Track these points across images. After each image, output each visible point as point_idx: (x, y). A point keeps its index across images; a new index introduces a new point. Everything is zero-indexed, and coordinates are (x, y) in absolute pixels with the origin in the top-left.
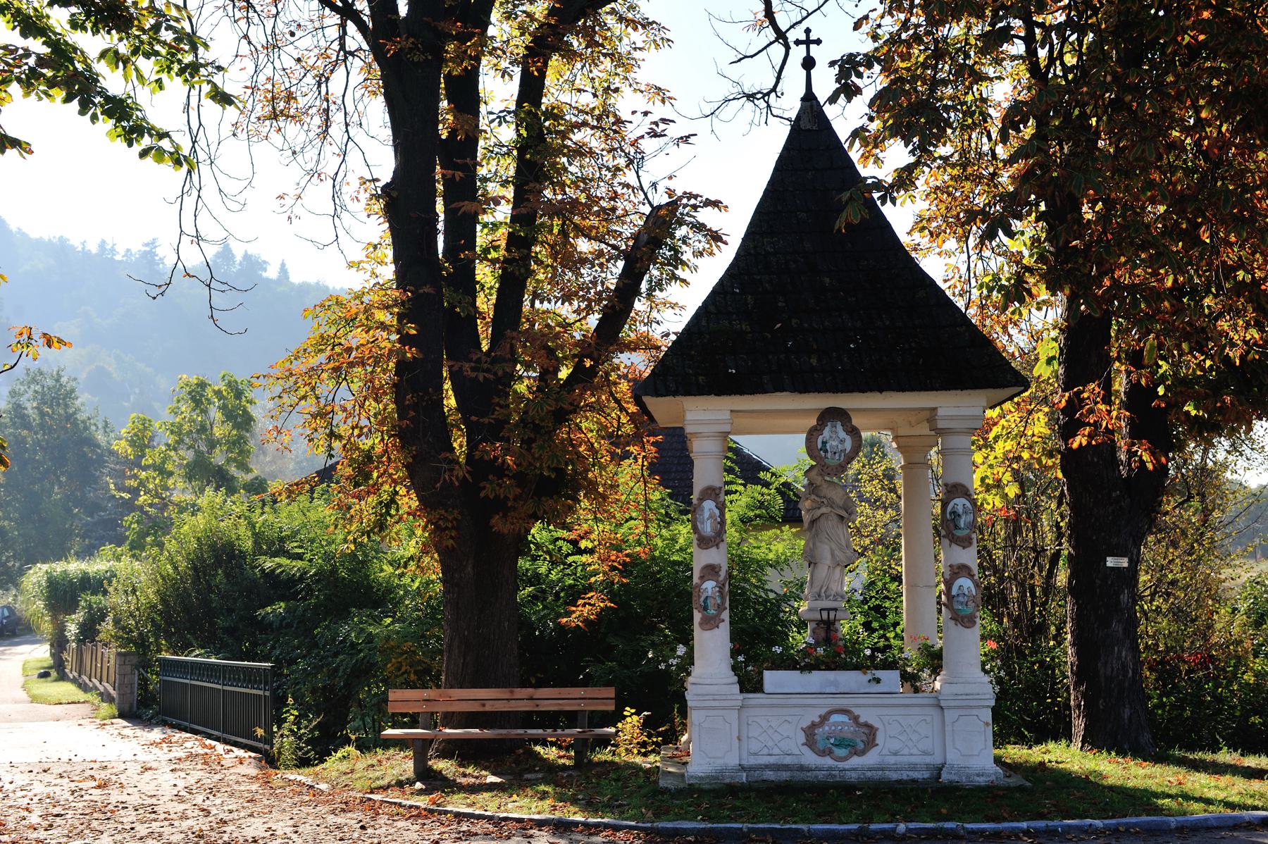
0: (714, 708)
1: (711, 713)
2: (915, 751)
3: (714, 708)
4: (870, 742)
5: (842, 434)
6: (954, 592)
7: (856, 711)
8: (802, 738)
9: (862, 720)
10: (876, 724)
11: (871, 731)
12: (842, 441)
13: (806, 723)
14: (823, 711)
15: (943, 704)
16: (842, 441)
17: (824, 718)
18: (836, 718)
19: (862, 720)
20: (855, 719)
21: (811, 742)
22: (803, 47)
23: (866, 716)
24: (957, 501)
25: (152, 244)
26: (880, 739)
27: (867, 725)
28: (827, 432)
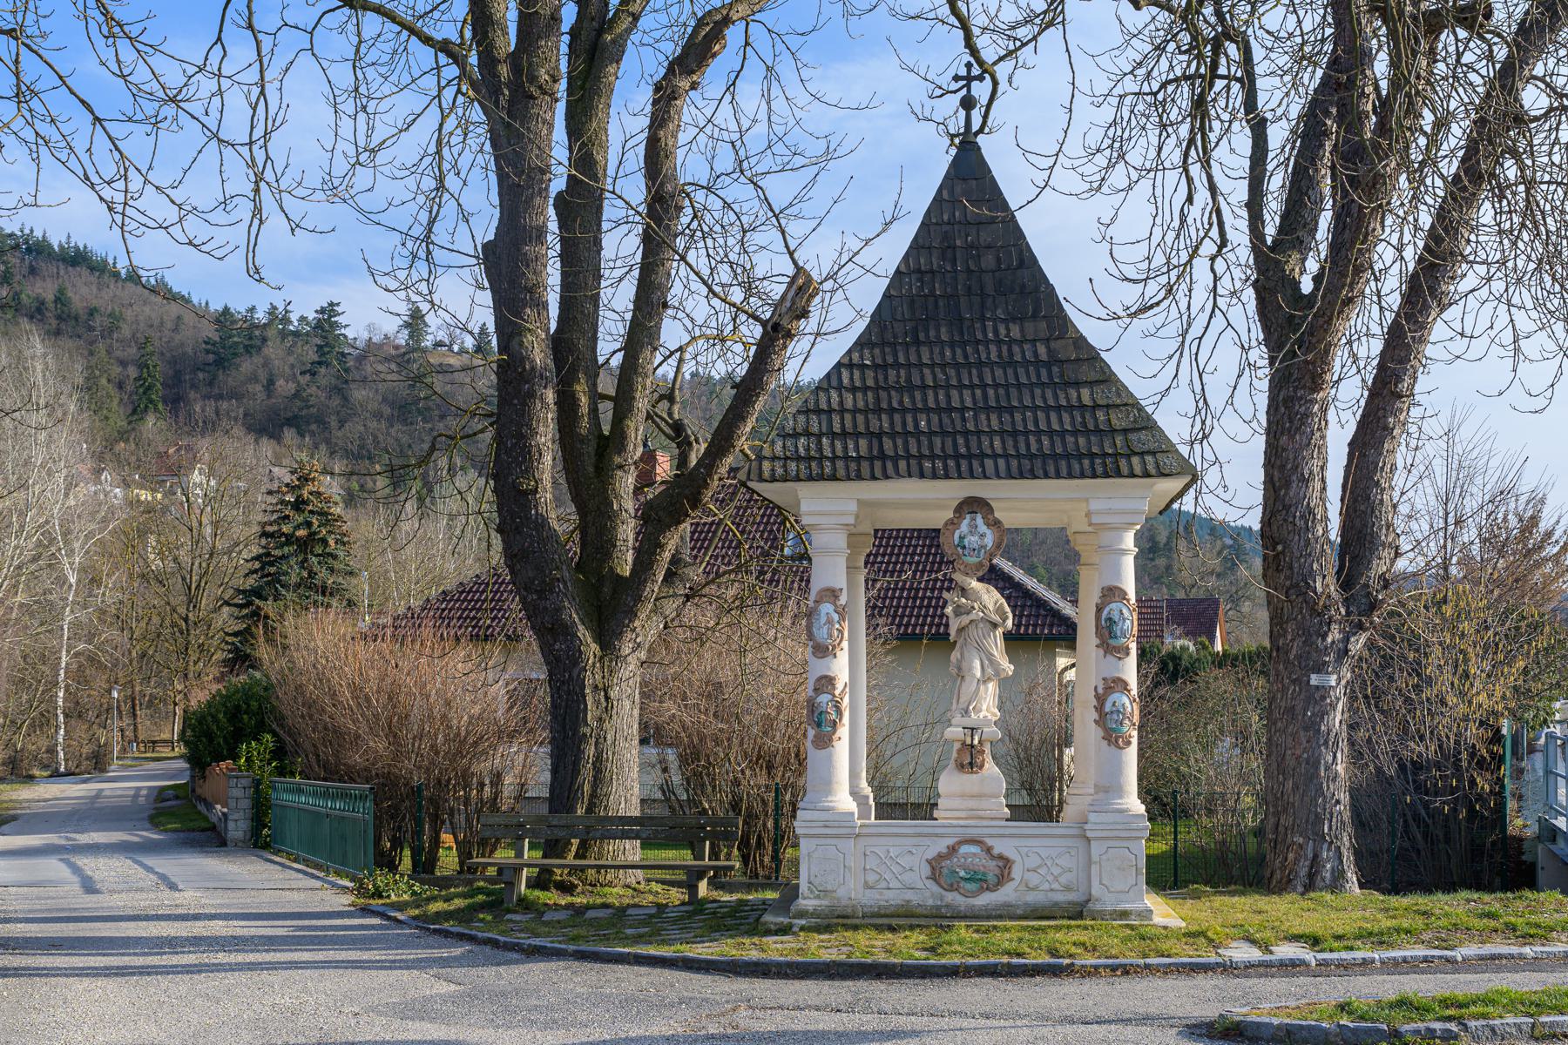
0: (826, 836)
1: (822, 841)
2: (1055, 886)
3: (826, 836)
4: (1003, 877)
5: (982, 528)
6: (1108, 708)
7: (990, 842)
8: (926, 870)
9: (996, 852)
10: (1010, 853)
11: (1005, 863)
12: (982, 536)
13: (931, 854)
14: (951, 841)
15: (1089, 834)
16: (982, 536)
17: (953, 850)
18: (964, 849)
19: (996, 852)
20: (989, 850)
21: (935, 876)
22: (224, 72)
23: (999, 847)
24: (1113, 606)
25: (252, 309)
26: (1016, 872)
27: (1001, 857)
28: (964, 526)
